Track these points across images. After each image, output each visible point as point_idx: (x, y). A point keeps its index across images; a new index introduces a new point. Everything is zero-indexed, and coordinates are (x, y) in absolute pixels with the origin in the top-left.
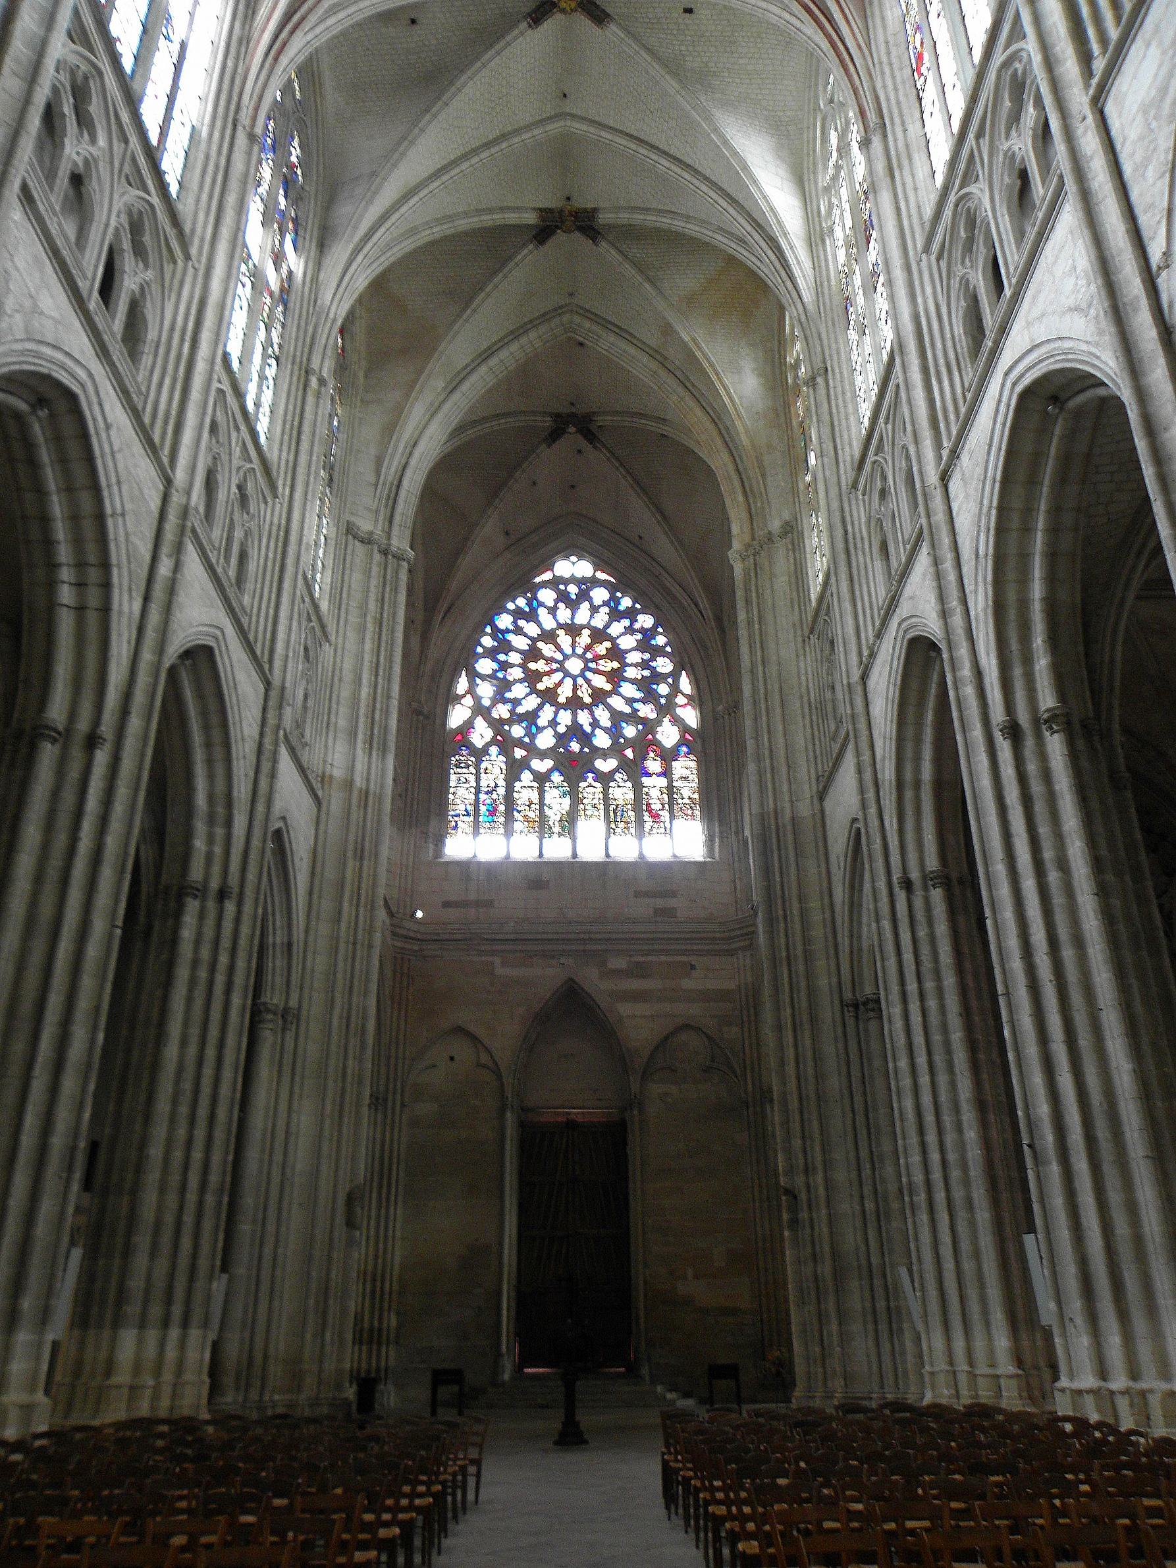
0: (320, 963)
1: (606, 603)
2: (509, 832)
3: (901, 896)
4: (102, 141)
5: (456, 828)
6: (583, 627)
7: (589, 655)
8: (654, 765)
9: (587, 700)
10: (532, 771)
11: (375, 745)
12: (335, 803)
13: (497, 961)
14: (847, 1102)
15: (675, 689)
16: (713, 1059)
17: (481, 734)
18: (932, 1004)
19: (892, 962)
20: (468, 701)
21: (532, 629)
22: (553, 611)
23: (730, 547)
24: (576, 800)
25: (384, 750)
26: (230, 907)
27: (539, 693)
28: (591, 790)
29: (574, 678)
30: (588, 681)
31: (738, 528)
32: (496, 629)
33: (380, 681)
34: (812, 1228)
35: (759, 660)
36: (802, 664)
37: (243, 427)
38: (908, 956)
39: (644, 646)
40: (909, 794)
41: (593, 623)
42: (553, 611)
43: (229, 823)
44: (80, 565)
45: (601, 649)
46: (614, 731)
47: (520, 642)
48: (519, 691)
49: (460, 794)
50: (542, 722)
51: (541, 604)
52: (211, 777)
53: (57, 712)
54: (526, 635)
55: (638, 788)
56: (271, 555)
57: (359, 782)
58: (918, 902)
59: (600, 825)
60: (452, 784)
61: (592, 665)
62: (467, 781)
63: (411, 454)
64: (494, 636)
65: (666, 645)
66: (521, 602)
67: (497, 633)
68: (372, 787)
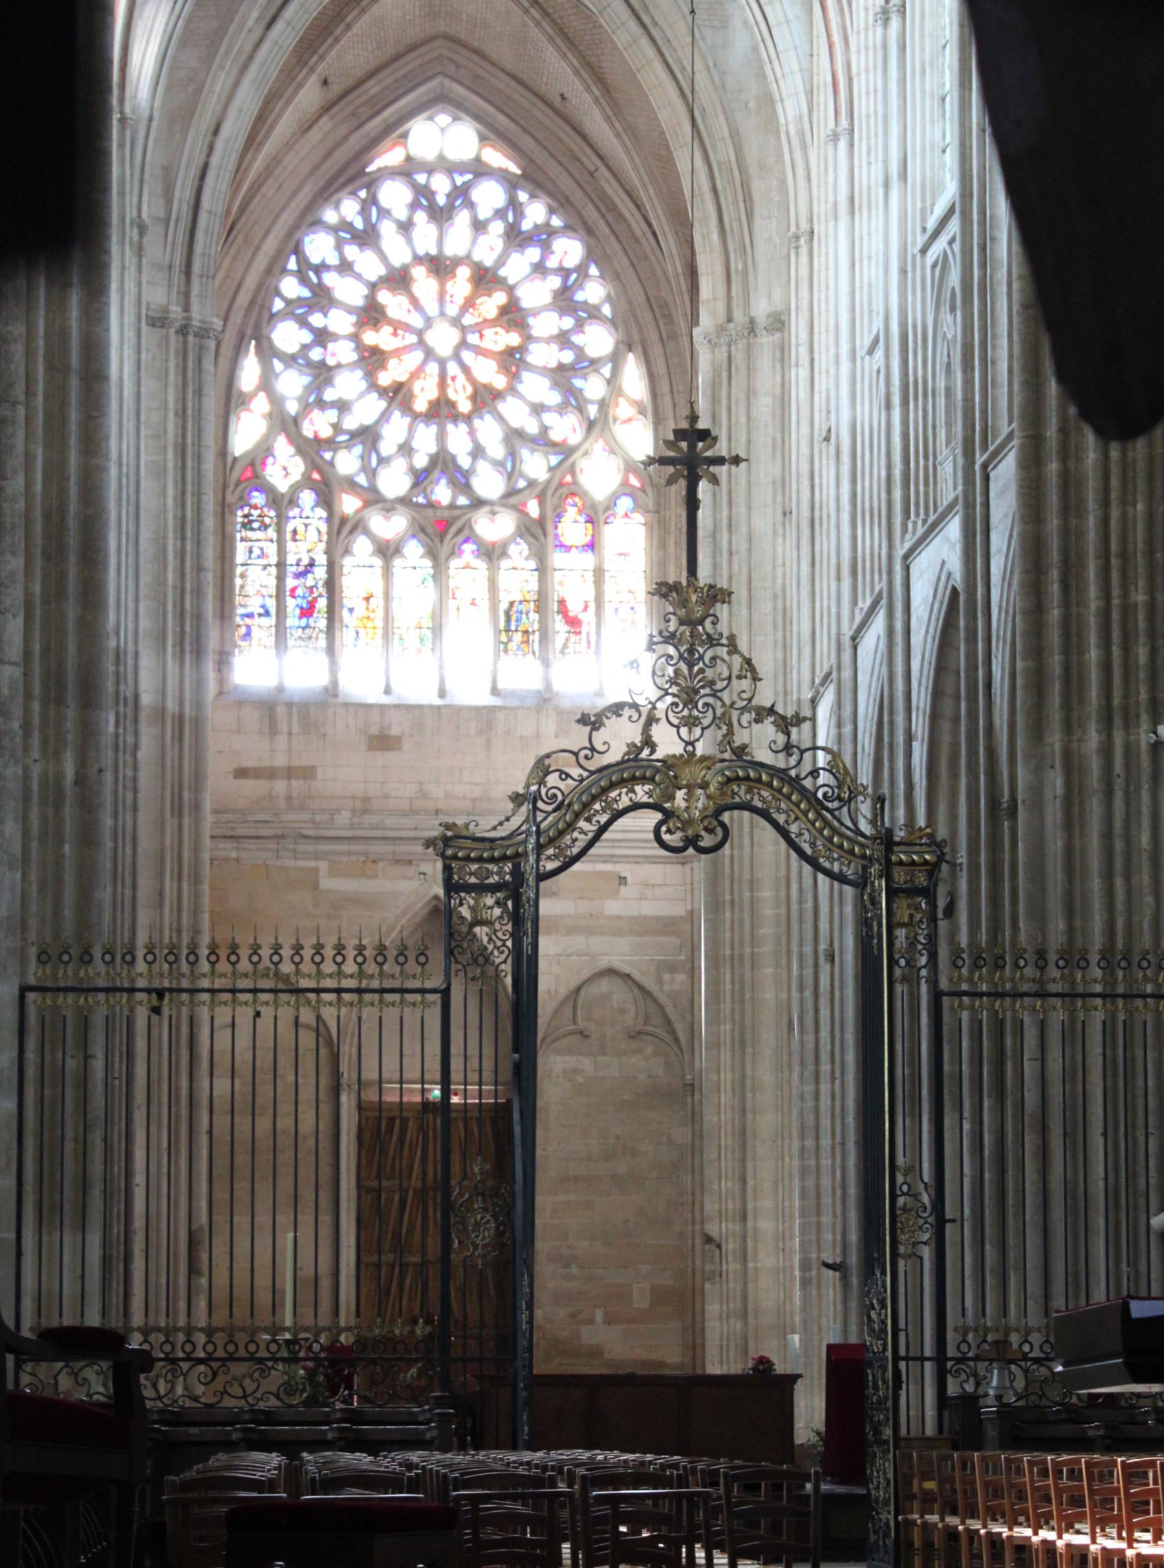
1: (500, 214)
3: (825, 968)
5: (248, 634)
6: (457, 262)
8: (572, 528)
11: (188, 648)
13: (323, 866)
16: (646, 1020)
20: (261, 404)
22: (406, 227)
30: (466, 370)
33: (189, 547)
35: (725, 522)
36: (780, 549)
38: (824, 1034)
39: (564, 300)
41: (476, 257)
42: (406, 227)
45: (491, 304)
46: (510, 468)
47: (349, 291)
50: (387, 447)
51: (384, 213)
57: (171, 706)
62: (263, 555)
63: (211, 148)
64: (304, 281)
66: (349, 209)
67: (307, 271)
68: (187, 711)
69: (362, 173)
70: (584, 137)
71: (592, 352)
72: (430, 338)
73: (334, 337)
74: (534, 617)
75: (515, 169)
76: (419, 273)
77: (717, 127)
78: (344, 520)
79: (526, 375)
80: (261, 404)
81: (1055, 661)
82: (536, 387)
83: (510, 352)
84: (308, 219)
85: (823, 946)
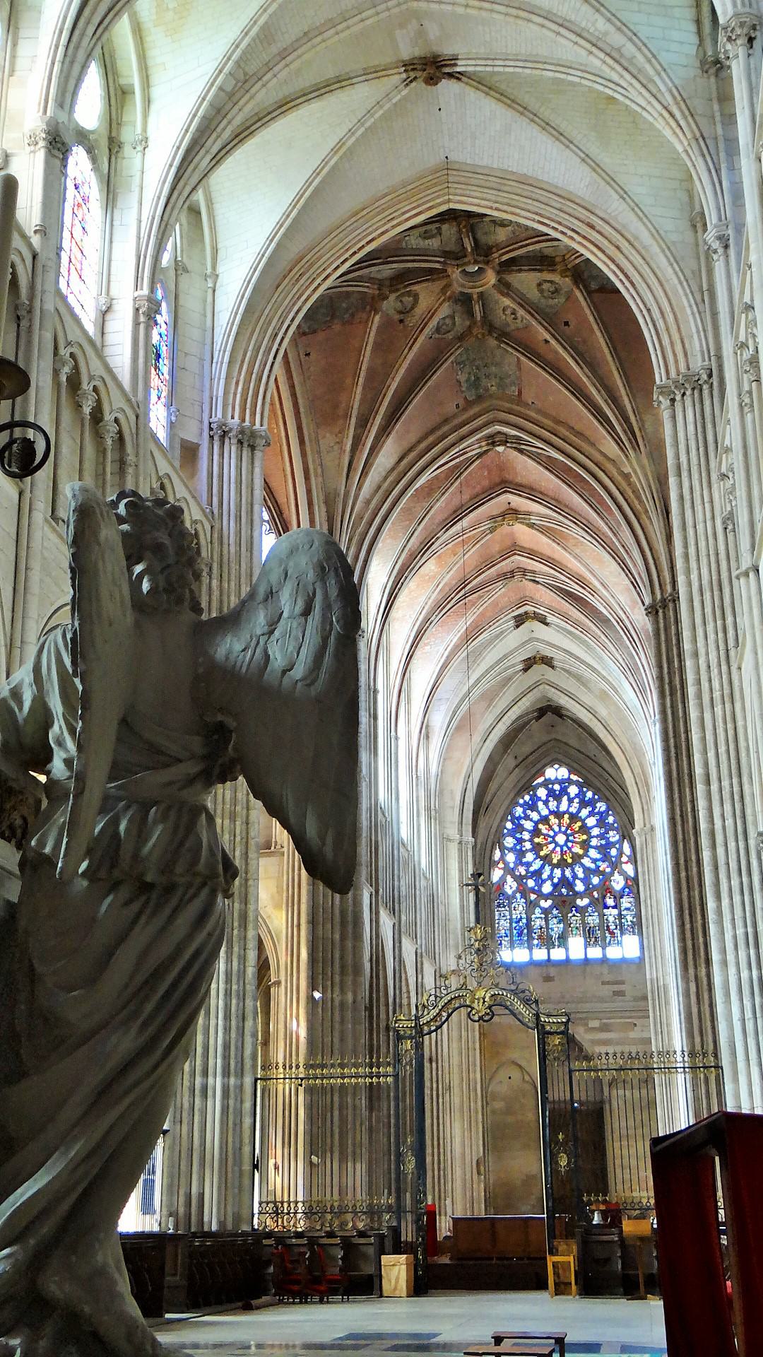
1: (577, 796)
2: (530, 948)
5: (501, 944)
6: (565, 813)
9: (570, 861)
10: (541, 908)
15: (621, 853)
17: (511, 886)
21: (535, 816)
22: (546, 803)
28: (573, 918)
29: (562, 847)
41: (571, 810)
42: (546, 803)
46: (586, 881)
47: (528, 825)
48: (530, 857)
49: (503, 925)
50: (545, 876)
51: (539, 799)
54: (531, 820)
55: (602, 916)
59: (582, 940)
60: (497, 918)
61: (571, 838)
72: (557, 839)
73: (525, 841)
76: (552, 817)
77: (635, 763)
78: (531, 902)
79: (590, 850)
80: (501, 865)
81: (689, 943)
82: (593, 853)
83: (584, 841)
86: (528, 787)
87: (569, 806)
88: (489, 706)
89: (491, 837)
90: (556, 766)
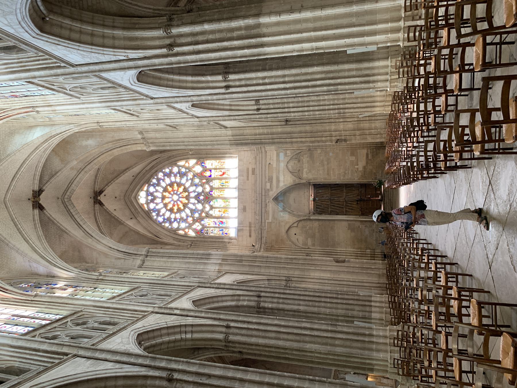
0: (273, 271)
1: (155, 187)
2: (228, 218)
3: (261, 111)
4: (59, 333)
5: (226, 234)
6: (163, 195)
7: (172, 193)
9: (187, 194)
11: (208, 257)
12: (227, 268)
13: (267, 221)
14: (313, 125)
15: (183, 166)
17: (198, 226)
18: (291, 105)
19: (279, 115)
20: (187, 230)
22: (157, 204)
23: (146, 150)
24: (218, 197)
25: (210, 254)
26: (263, 294)
27: (184, 208)
30: (181, 193)
31: (139, 148)
32: (163, 222)
33: (188, 256)
34: (347, 136)
36: (185, 131)
37: (123, 296)
38: (278, 111)
40: (233, 108)
41: (162, 192)
42: (157, 204)
43: (239, 295)
44: (181, 332)
45: (170, 189)
47: (168, 214)
49: (216, 232)
50: (194, 208)
52: (226, 301)
53: (221, 336)
54: (165, 212)
56: (159, 288)
57: (219, 262)
58: (263, 107)
60: (213, 235)
62: (212, 230)
65: (169, 169)
66: (154, 214)
69: (147, 211)
70: (140, 172)
71: (177, 171)
73: (175, 217)
74: (223, 181)
75: (147, 185)
76: (164, 202)
77: (106, 147)
78: (206, 216)
80: (187, 230)
82: (184, 181)
83: (177, 185)
84: (155, 222)
85: (256, 112)
86: (148, 214)
87: (159, 192)
88: (66, 233)
89: (172, 235)
90: (139, 197)
